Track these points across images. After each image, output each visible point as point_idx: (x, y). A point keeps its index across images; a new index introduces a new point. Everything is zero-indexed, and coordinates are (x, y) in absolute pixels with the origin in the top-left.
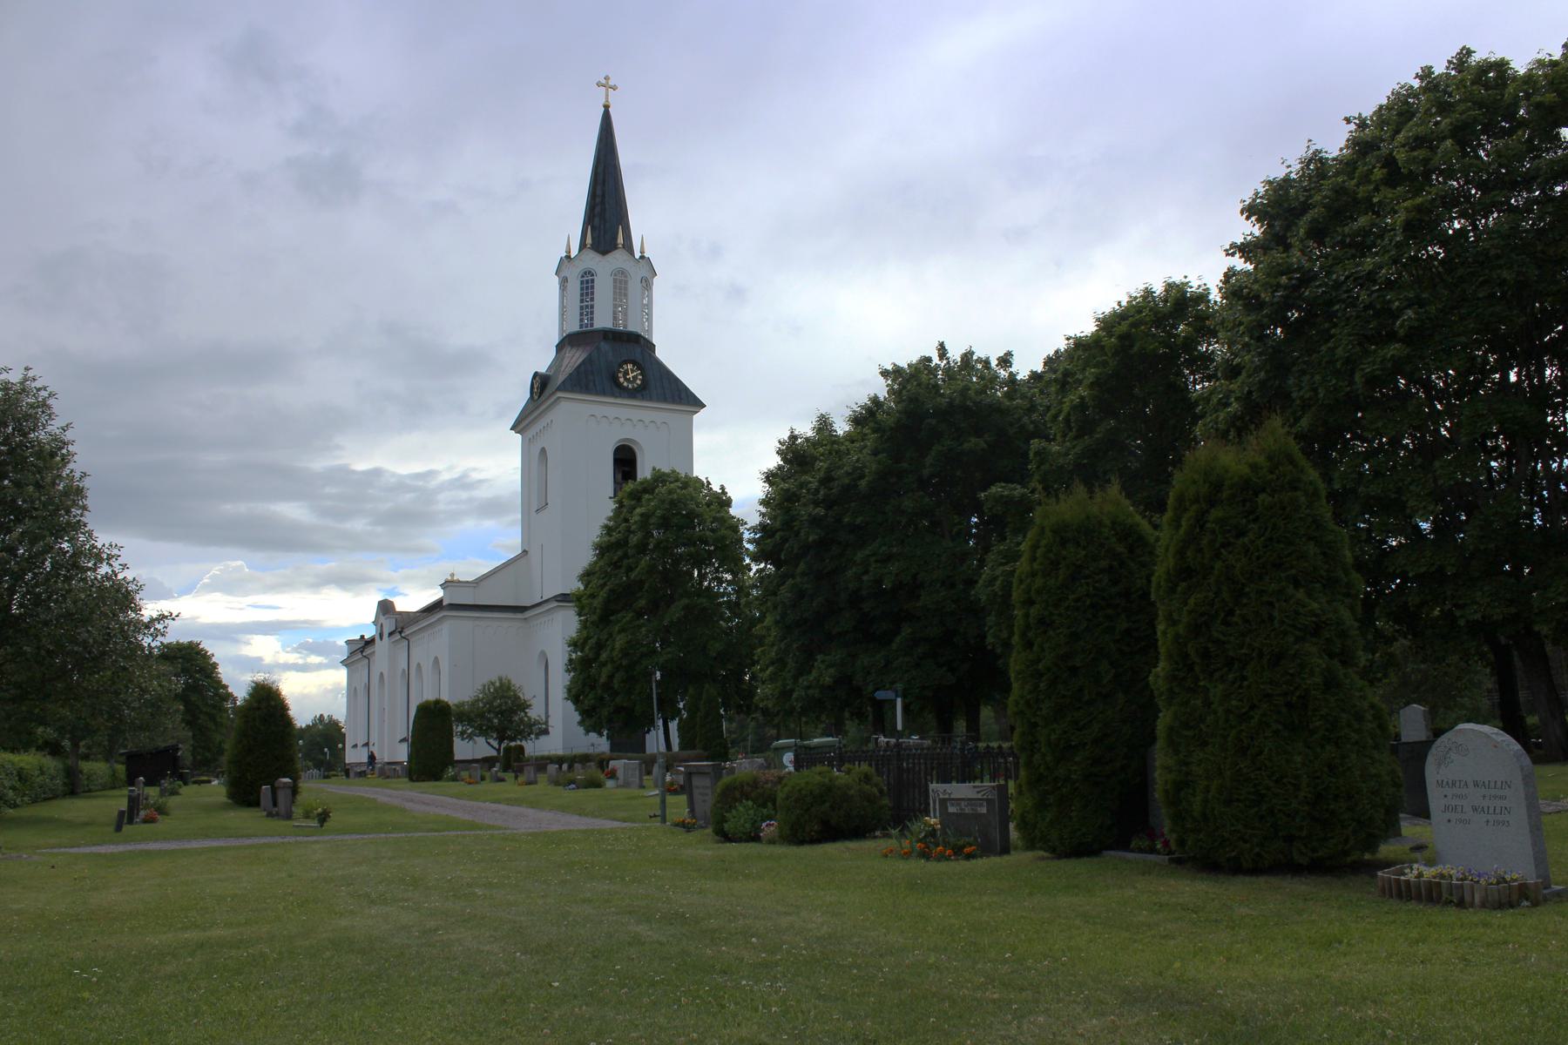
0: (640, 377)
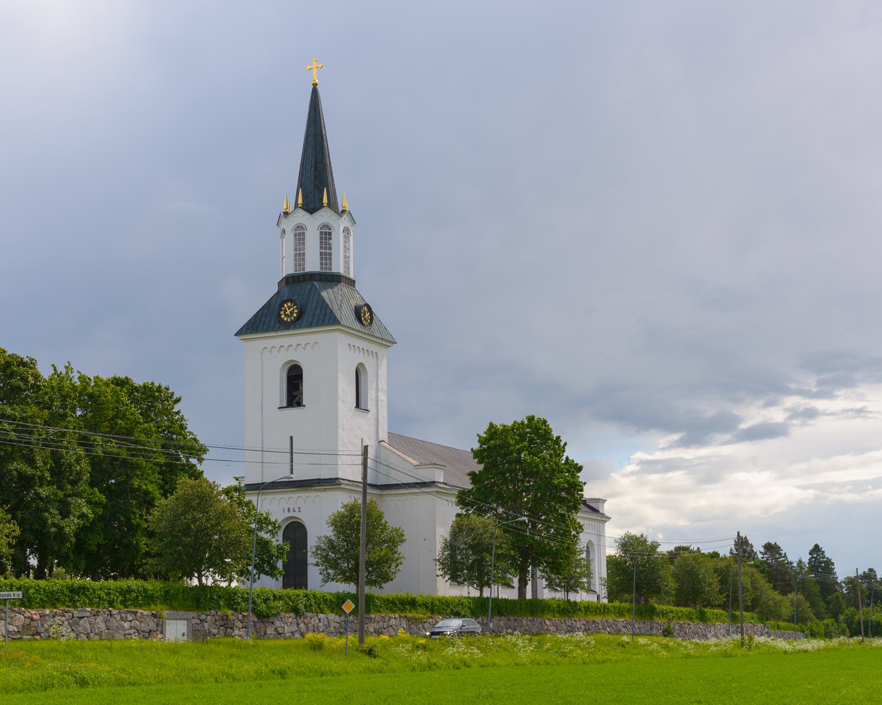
0: (296, 311)
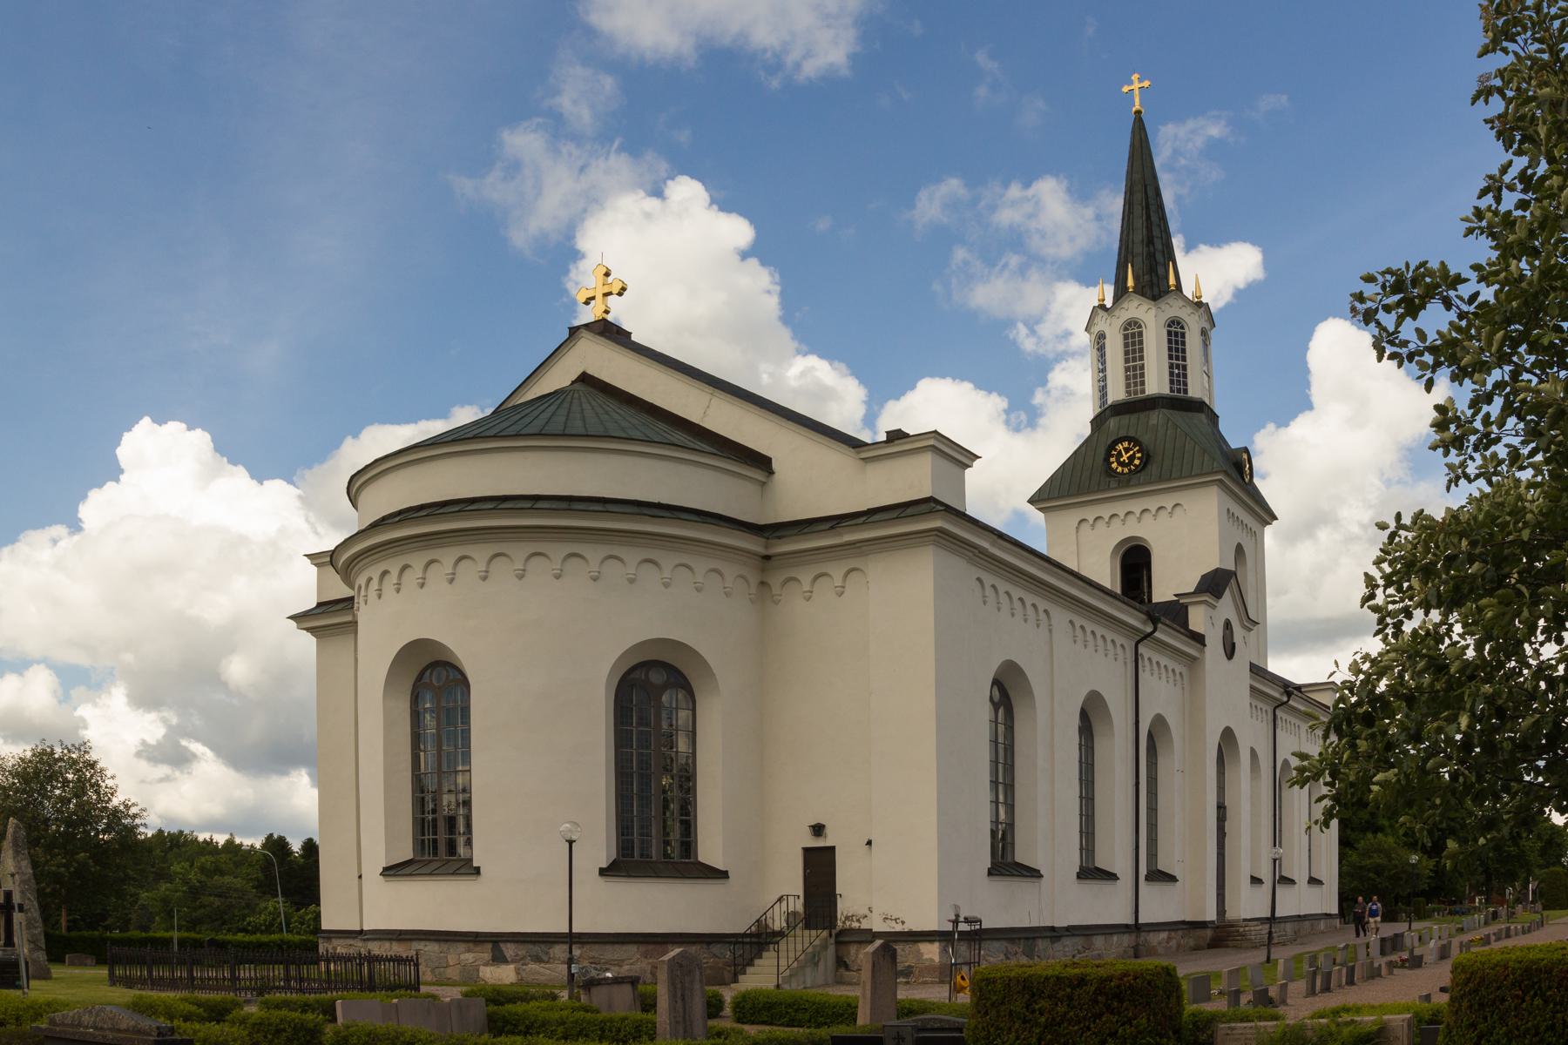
0: (1139, 455)
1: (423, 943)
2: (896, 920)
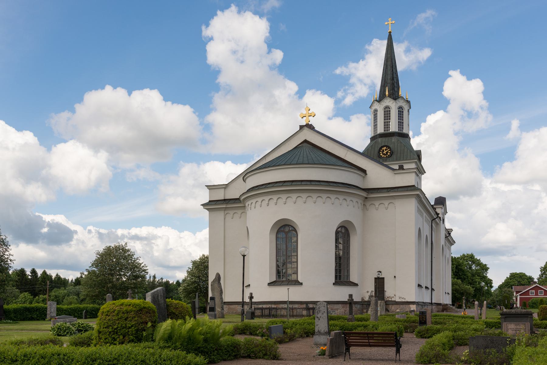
0: (389, 152)
1: (284, 305)
2: (403, 298)
